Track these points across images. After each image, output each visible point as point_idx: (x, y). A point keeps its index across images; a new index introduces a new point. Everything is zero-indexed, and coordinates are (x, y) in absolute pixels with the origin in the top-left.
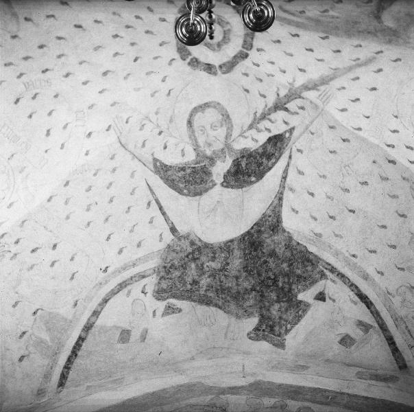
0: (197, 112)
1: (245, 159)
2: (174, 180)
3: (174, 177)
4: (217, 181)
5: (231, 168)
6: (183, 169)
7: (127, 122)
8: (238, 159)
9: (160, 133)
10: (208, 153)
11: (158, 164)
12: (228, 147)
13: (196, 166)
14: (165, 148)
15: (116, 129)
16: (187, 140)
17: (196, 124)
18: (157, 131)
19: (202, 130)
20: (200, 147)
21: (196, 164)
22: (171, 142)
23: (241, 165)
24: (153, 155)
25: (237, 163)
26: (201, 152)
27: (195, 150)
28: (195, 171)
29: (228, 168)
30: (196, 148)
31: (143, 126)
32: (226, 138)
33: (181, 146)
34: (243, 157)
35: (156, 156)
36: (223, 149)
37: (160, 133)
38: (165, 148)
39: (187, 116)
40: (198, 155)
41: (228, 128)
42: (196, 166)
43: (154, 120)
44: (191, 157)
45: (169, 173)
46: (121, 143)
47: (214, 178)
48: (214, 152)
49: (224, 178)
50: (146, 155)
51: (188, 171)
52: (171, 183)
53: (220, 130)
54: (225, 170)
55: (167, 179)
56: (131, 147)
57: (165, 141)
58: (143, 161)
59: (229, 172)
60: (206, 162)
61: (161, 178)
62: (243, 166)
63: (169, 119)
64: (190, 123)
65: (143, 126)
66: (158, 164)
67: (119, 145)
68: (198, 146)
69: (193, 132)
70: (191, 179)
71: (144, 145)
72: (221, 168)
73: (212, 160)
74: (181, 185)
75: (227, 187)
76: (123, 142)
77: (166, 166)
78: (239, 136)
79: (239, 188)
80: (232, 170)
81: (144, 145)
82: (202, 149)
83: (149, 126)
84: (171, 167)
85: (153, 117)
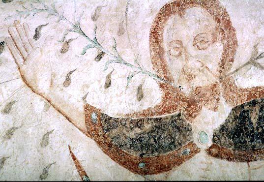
0: (169, 15)
1: (257, 108)
2: (121, 146)
3: (122, 140)
4: (199, 145)
5: (227, 121)
6: (138, 124)
7: (36, 36)
8: (242, 106)
9: (99, 57)
10: (187, 91)
11: (94, 116)
12: (225, 80)
13: (163, 116)
14: (108, 84)
15: (14, 49)
16: (149, 67)
17: (166, 36)
18: (93, 53)
19: (177, 48)
20: (172, 80)
21: (163, 112)
22: (119, 73)
23: (249, 118)
24: (84, 98)
25: (241, 115)
26: (174, 89)
27: (161, 86)
28: (159, 126)
29: (221, 121)
30: (165, 83)
31: (67, 43)
32: (222, 64)
33: (138, 79)
34: (254, 103)
35: (90, 101)
36: (215, 86)
37: (99, 57)
38: (108, 84)
39: (150, 21)
40: (167, 97)
41: (227, 48)
42: (163, 116)
43: (89, 32)
44: (155, 97)
45: (114, 132)
46: (24, 80)
47: (195, 137)
48: (197, 91)
49: (214, 140)
50: (73, 99)
51: (148, 127)
52: (112, 149)
53: (210, 49)
54: (217, 125)
55: (110, 145)
56: (43, 86)
57: (108, 72)
58: (66, 113)
59: (223, 129)
60: (181, 108)
61: (99, 143)
62: (254, 121)
63: (117, 28)
64: (155, 35)
65: (67, 43)
66: (94, 116)
67: (20, 82)
68: (169, 79)
69: (160, 53)
70: (152, 141)
71: (68, 81)
72: (210, 120)
73: (192, 104)
74: (134, 155)
75: (217, 156)
76: (29, 77)
77: (108, 119)
78: (249, 63)
79: (242, 160)
80: (231, 126)
81: (68, 81)
82: (175, 84)
83: (76, 47)
84: (116, 120)
85: (88, 25)
